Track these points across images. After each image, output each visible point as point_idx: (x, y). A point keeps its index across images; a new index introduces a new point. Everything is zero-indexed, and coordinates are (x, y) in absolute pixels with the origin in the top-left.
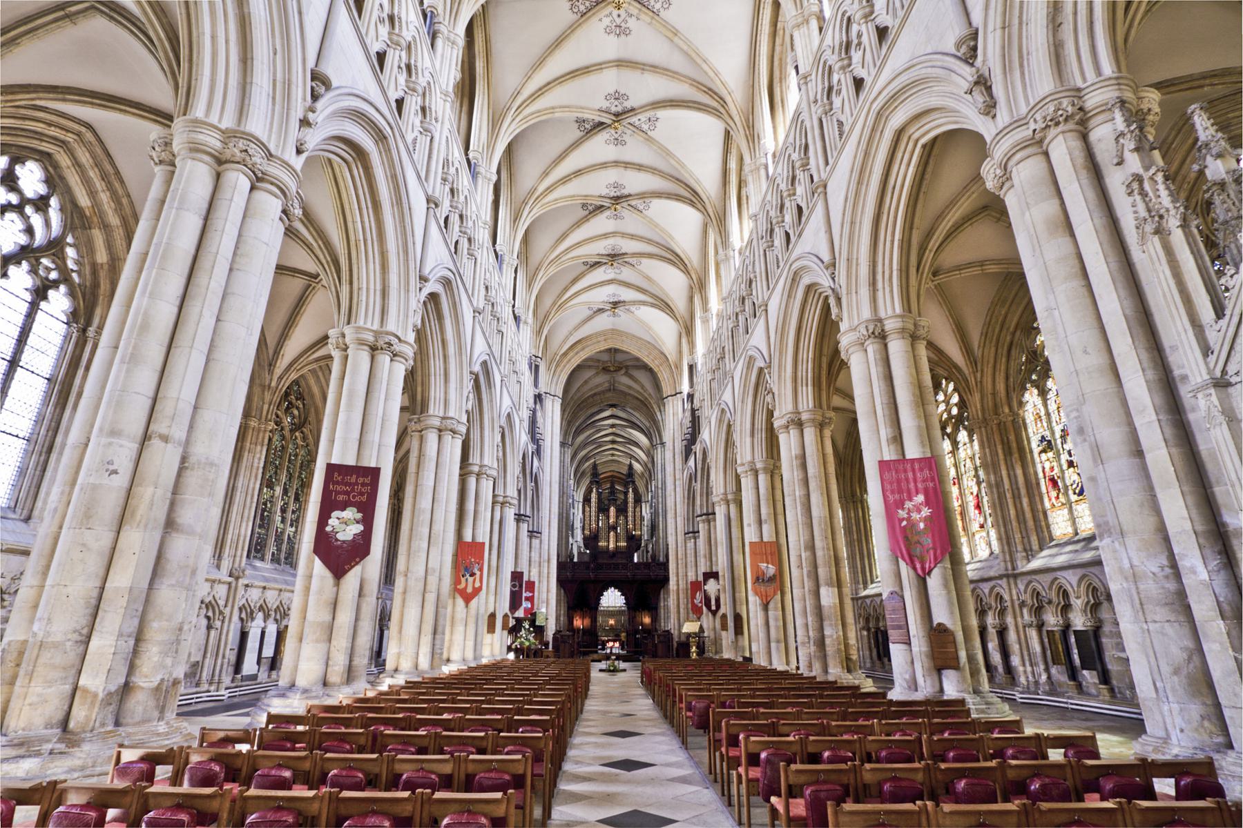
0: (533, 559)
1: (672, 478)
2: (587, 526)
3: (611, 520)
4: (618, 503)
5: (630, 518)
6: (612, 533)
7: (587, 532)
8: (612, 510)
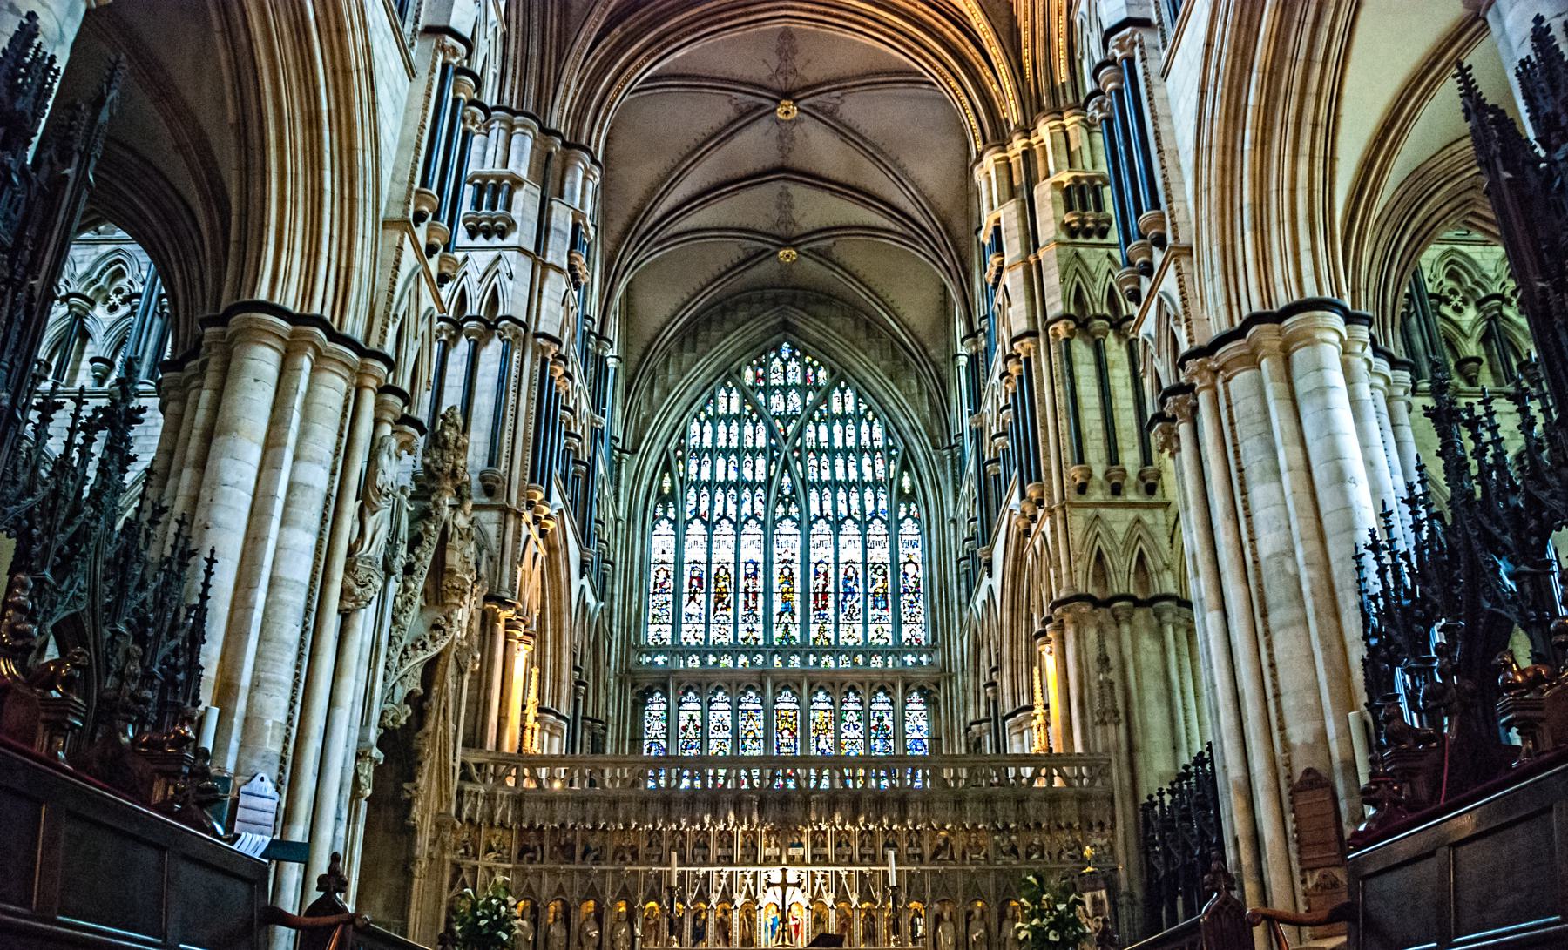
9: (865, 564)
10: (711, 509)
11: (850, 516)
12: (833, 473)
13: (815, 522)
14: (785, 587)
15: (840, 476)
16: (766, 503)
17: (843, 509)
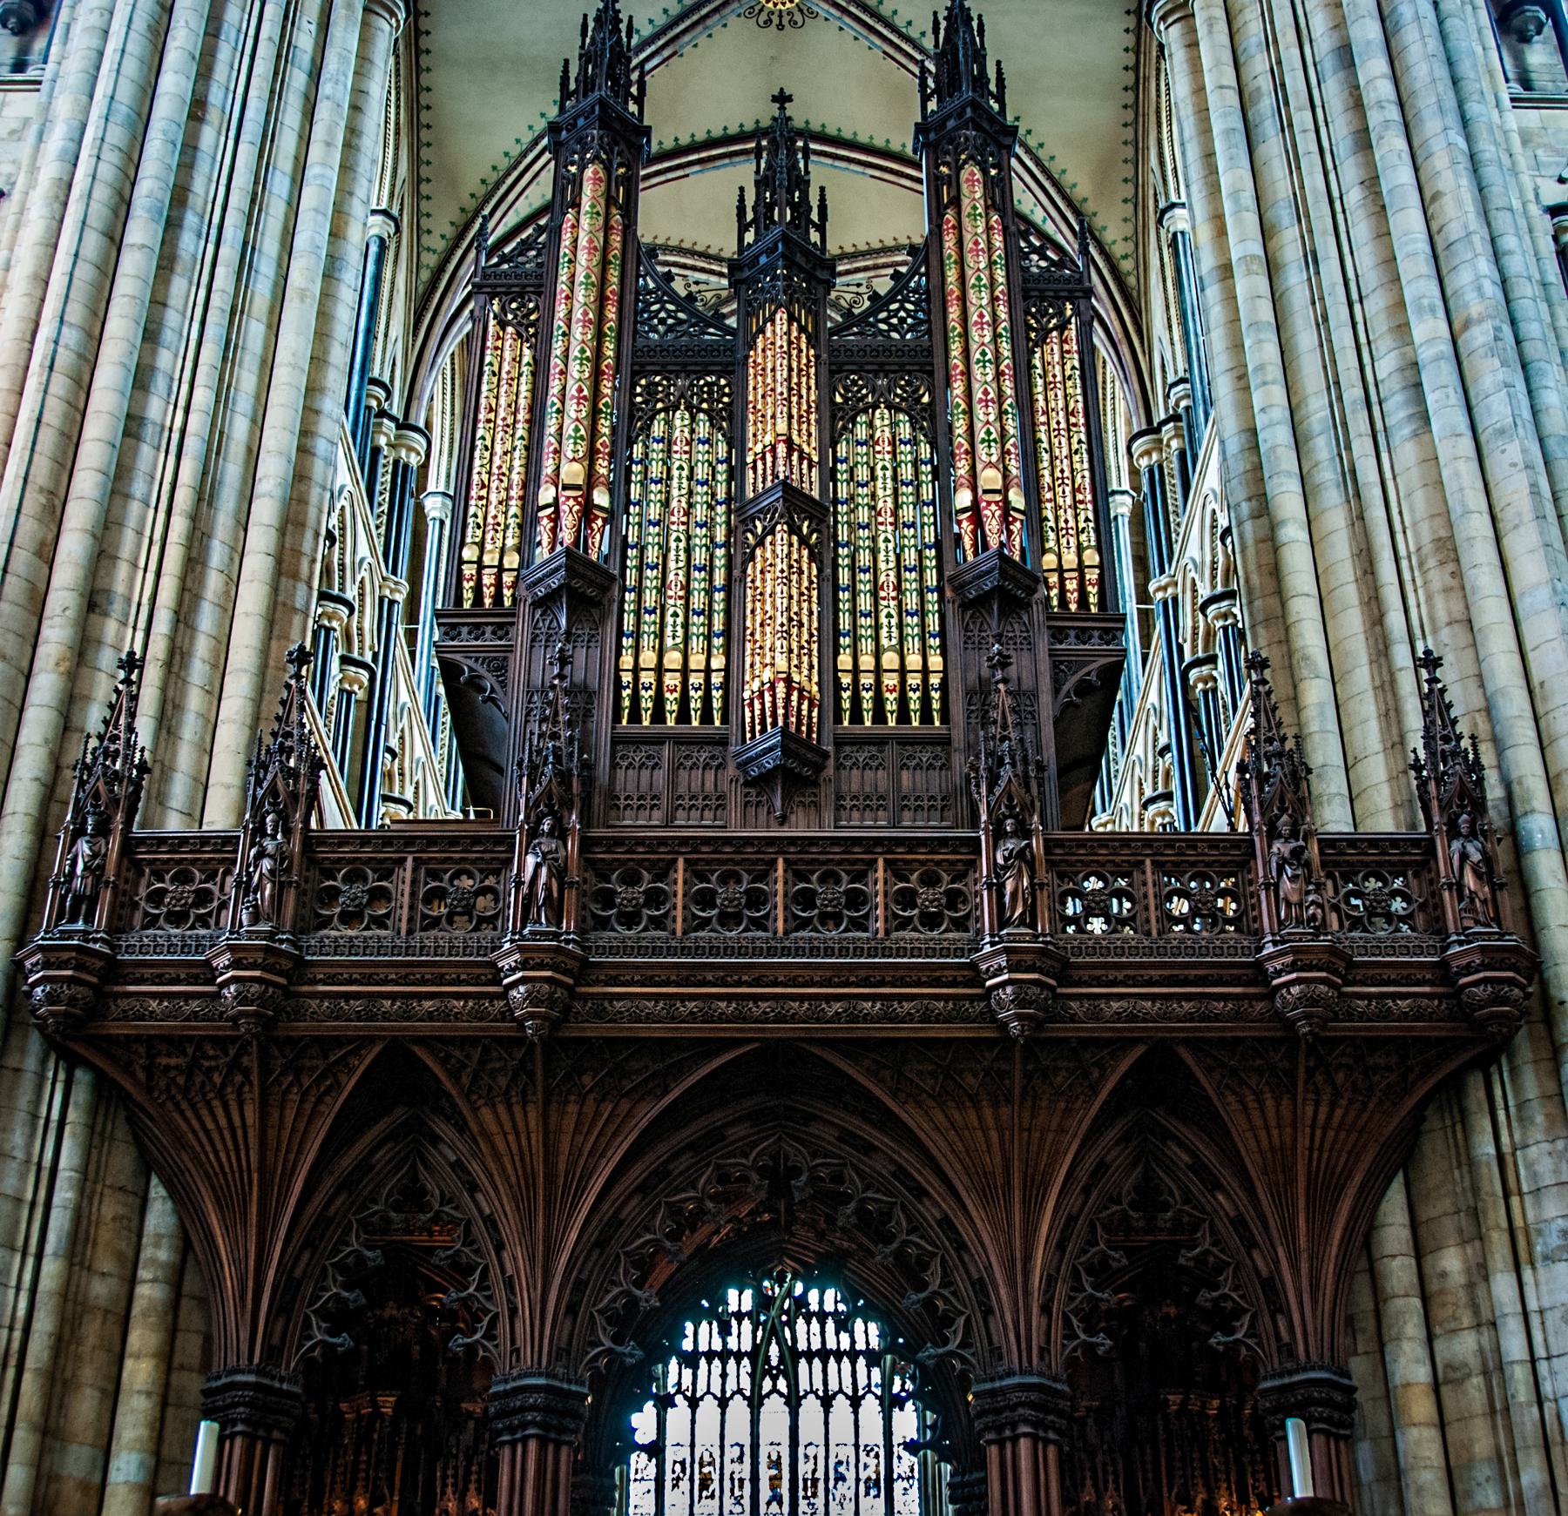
9: (857, 1446)
10: (694, 1383)
11: (841, 1391)
12: (824, 1342)
13: (805, 1397)
14: (774, 1472)
15: (831, 1344)
16: (752, 1375)
17: (833, 1386)
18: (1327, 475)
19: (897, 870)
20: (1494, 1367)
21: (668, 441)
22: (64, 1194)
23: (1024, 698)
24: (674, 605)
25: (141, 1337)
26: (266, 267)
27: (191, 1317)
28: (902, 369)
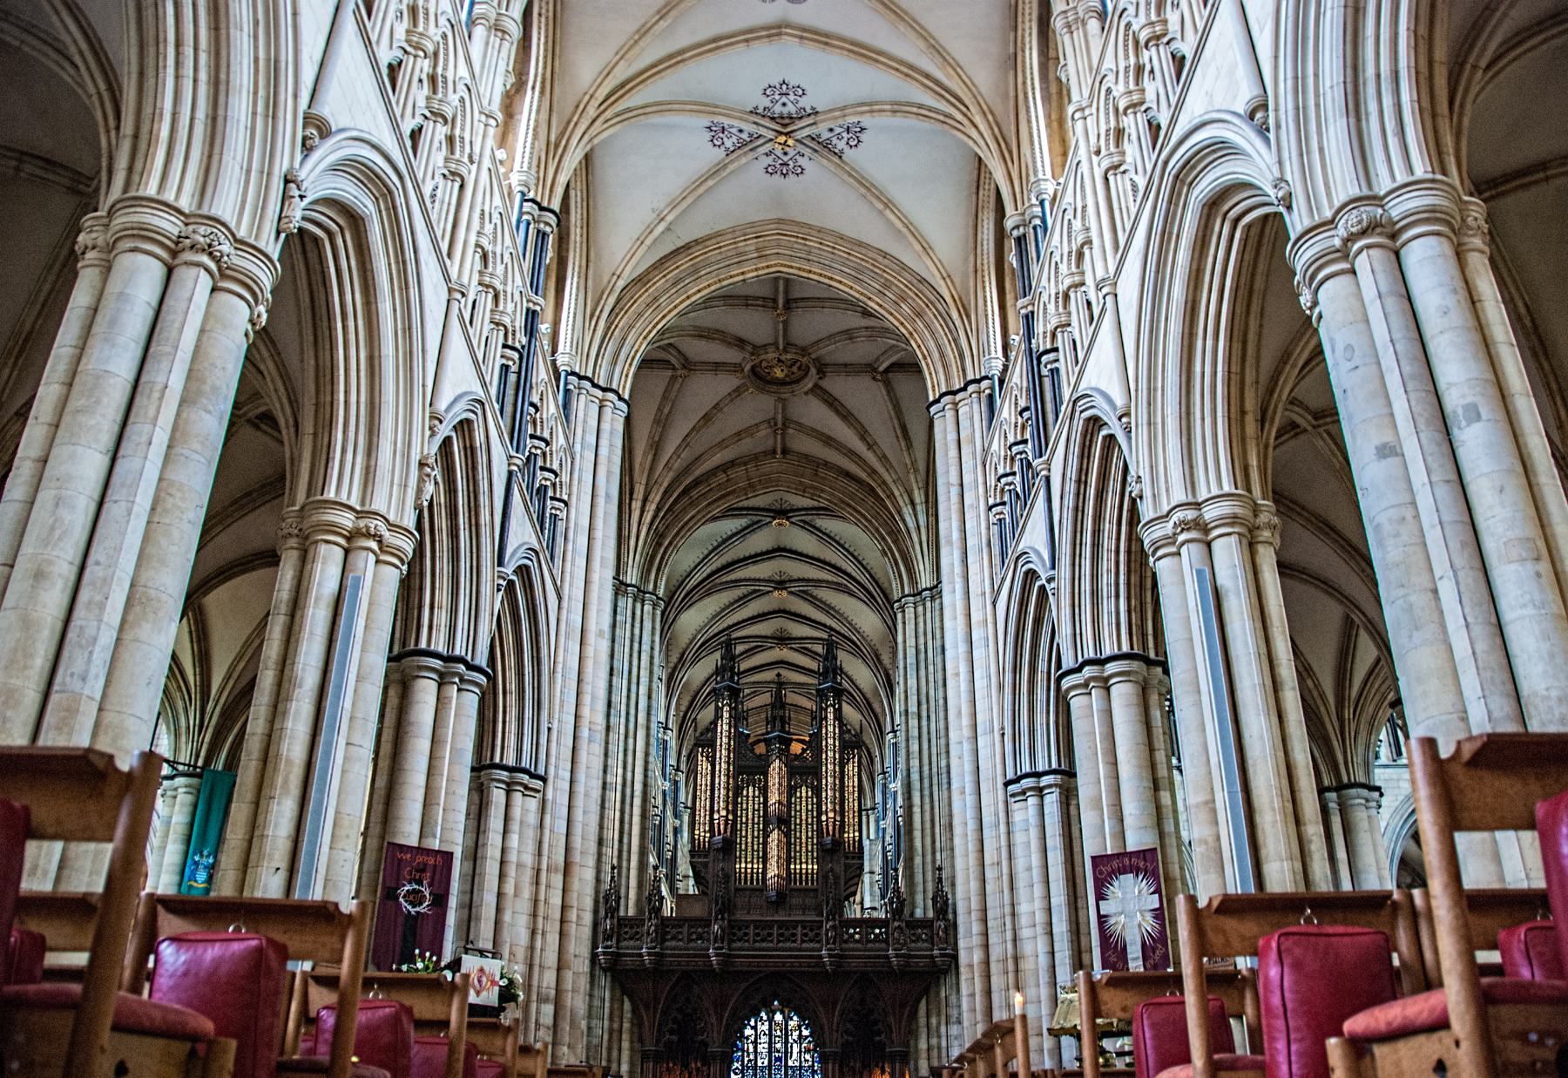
0: (513, 857)
1: (961, 620)
2: (702, 816)
3: (773, 798)
4: (796, 748)
5: (828, 794)
6: (775, 835)
7: (702, 832)
8: (776, 768)
18: (927, 792)
19: (804, 927)
20: (939, 1048)
21: (747, 796)
22: (607, 1004)
23: (837, 878)
24: (749, 849)
25: (625, 1036)
26: (632, 719)
27: (635, 1029)
28: (810, 774)
